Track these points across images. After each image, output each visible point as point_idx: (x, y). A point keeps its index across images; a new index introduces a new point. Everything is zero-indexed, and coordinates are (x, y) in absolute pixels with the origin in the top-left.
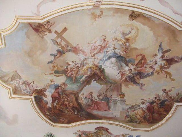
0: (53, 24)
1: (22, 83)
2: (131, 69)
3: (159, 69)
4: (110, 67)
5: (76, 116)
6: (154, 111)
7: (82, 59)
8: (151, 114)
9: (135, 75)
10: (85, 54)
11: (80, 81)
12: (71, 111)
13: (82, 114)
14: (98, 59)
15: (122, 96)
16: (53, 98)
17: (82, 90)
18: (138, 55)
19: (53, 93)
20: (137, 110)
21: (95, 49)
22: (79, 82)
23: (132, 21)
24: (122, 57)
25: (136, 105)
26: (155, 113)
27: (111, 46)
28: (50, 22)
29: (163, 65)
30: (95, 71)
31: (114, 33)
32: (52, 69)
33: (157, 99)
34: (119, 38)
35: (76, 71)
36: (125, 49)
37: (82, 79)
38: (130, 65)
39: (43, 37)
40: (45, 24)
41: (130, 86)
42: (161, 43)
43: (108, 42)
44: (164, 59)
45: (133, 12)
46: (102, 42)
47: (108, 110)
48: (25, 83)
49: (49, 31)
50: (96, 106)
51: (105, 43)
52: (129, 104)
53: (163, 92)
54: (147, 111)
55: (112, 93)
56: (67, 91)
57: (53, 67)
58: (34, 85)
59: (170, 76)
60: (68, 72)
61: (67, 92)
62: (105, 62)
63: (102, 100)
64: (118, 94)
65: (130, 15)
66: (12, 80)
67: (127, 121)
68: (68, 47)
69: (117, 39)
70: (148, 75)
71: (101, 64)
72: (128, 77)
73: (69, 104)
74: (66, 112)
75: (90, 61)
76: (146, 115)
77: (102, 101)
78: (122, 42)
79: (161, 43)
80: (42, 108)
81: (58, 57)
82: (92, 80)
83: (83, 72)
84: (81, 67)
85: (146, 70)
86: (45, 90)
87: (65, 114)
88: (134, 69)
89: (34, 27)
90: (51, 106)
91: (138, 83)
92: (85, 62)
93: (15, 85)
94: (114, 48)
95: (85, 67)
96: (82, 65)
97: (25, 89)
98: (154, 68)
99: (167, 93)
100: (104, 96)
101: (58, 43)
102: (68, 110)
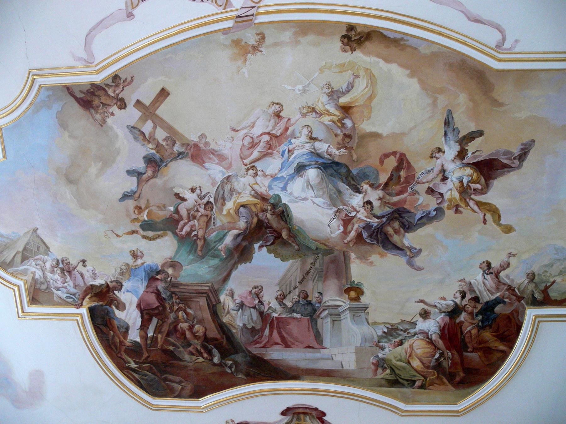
0: (129, 84)
1: (53, 267)
2: (369, 203)
3: (456, 195)
4: (305, 199)
5: (215, 369)
6: (463, 340)
7: (219, 178)
8: (456, 353)
9: (384, 219)
10: (224, 163)
11: (217, 249)
12: (201, 355)
13: (236, 363)
14: (265, 176)
15: (353, 294)
16: (142, 312)
17: (226, 279)
18: (386, 156)
20: (411, 341)
21: (253, 145)
22: (216, 252)
23: (350, 52)
24: (337, 164)
25: (403, 321)
26: (470, 350)
27: (301, 132)
28: (120, 78)
29: (468, 182)
30: (261, 215)
31: (304, 91)
32: (134, 216)
33: (469, 296)
34: (320, 107)
35: (205, 219)
36: (343, 140)
37: (224, 243)
38: (365, 187)
39: (105, 122)
40: (107, 85)
41: (374, 258)
42: (450, 113)
43: (289, 119)
44: (464, 161)
45: (351, 27)
46: (273, 121)
47: (314, 344)
48: (61, 265)
49: (119, 103)
50: (275, 333)
51: (282, 124)
52: (380, 319)
53: (484, 271)
54: (440, 343)
55: (320, 284)
56: (181, 285)
57: (136, 212)
58: (87, 272)
59: (497, 218)
60: (182, 223)
62: (287, 184)
63: (292, 310)
64: (340, 289)
65: (344, 37)
66: (24, 259)
67: (384, 382)
68: (173, 145)
69: (313, 110)
70: (427, 219)
71: (277, 192)
72: (364, 228)
73: (191, 328)
74: (187, 357)
75: (241, 185)
76: (442, 355)
77: (295, 315)
78: (331, 118)
79: (450, 113)
81: (149, 179)
82: (256, 246)
83: (225, 220)
84: (219, 205)
85: (418, 199)
86: (119, 286)
87: (182, 363)
88: (380, 199)
89: (79, 95)
90: (138, 339)
91: (398, 248)
92: (227, 187)
93: (34, 273)
94: (311, 138)
95: (230, 205)
96: (221, 199)
97: (62, 285)
98: (441, 194)
99: (497, 275)
100: (299, 296)
101: (147, 136)
102: (191, 349)
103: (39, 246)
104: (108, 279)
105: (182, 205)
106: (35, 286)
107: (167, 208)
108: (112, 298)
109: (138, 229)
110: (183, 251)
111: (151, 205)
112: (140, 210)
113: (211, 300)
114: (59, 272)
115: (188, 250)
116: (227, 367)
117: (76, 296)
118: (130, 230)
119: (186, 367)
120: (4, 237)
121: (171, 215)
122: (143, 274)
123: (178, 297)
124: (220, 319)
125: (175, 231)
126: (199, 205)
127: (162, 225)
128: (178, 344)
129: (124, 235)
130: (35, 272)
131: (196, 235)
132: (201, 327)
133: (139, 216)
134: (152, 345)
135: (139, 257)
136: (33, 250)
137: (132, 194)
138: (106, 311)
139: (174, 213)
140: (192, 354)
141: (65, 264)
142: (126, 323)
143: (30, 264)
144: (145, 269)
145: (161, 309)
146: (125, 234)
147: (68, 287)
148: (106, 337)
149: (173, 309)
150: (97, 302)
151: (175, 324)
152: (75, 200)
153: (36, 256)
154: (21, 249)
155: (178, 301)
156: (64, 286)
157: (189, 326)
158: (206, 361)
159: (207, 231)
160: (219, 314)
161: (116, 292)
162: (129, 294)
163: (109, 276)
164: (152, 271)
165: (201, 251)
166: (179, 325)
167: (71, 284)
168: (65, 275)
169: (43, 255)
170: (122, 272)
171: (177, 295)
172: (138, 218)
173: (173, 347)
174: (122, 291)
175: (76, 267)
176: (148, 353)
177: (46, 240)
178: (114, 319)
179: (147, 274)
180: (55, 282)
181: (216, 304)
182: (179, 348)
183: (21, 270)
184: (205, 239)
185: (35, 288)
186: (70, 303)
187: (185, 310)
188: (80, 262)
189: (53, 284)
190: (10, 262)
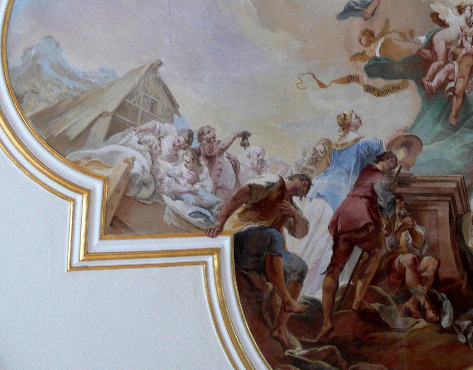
1: (177, 147)
5: (443, 340)
16: (336, 237)
19: (345, 204)
32: (358, 49)
57: (363, 41)
60: (434, 66)
61: (415, 187)
73: (416, 262)
74: (399, 321)
80: (267, 317)
87: (390, 335)
90: (319, 295)
93: (130, 162)
102: (409, 304)
103: (156, 102)
104: (285, 173)
105: (439, 33)
106: (126, 190)
107: (415, 38)
108: (284, 212)
109: (360, 74)
110: (428, 117)
111: (390, 30)
112: (371, 39)
113: (455, 207)
114: (187, 158)
115: (436, 115)
116: (460, 331)
117: (214, 211)
118: (345, 75)
119: (395, 341)
120: (79, 80)
121: (420, 51)
122: (354, 161)
123: (405, 204)
124: (464, 242)
125: (422, 80)
126: (466, 36)
127: (402, 69)
128: (388, 296)
129: (333, 84)
130: (133, 159)
131: (453, 89)
132: (433, 260)
133: (367, 50)
134: (343, 303)
135: (352, 128)
136: (141, 108)
137: (361, 6)
138: (269, 240)
139: (425, 48)
140: (408, 313)
141: (205, 142)
142: (304, 262)
143: (127, 141)
144: (358, 152)
145: (371, 228)
146: (334, 82)
147: (201, 192)
148: (257, 297)
149: (392, 227)
150: (255, 221)
151: (391, 257)
152: (255, 10)
153: (146, 122)
154: (111, 108)
155: (403, 212)
156: (193, 189)
157: (414, 260)
158: (430, 324)
159: (470, 82)
160: (464, 232)
161: (295, 199)
162: (321, 201)
163: (290, 166)
164: (369, 155)
165: (456, 117)
166: (397, 259)
167: (209, 184)
168: (200, 165)
169: (161, 122)
170: (316, 158)
171: (404, 200)
172: (364, 52)
173: (379, 305)
174: (307, 196)
175: (227, 148)
176: (332, 322)
177: (174, 90)
178: (281, 256)
179: (361, 159)
180: (174, 180)
181: (462, 215)
182: (389, 304)
183: (102, 156)
184: (464, 96)
185: (124, 195)
186: (197, 228)
187: (412, 229)
188: (238, 136)
189: (169, 184)
190: (79, 136)
